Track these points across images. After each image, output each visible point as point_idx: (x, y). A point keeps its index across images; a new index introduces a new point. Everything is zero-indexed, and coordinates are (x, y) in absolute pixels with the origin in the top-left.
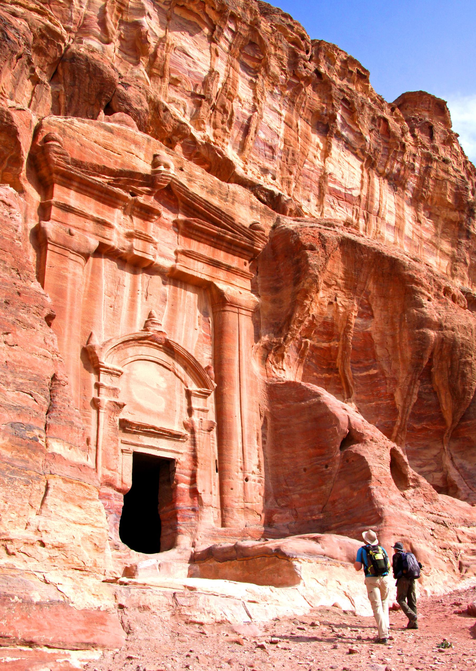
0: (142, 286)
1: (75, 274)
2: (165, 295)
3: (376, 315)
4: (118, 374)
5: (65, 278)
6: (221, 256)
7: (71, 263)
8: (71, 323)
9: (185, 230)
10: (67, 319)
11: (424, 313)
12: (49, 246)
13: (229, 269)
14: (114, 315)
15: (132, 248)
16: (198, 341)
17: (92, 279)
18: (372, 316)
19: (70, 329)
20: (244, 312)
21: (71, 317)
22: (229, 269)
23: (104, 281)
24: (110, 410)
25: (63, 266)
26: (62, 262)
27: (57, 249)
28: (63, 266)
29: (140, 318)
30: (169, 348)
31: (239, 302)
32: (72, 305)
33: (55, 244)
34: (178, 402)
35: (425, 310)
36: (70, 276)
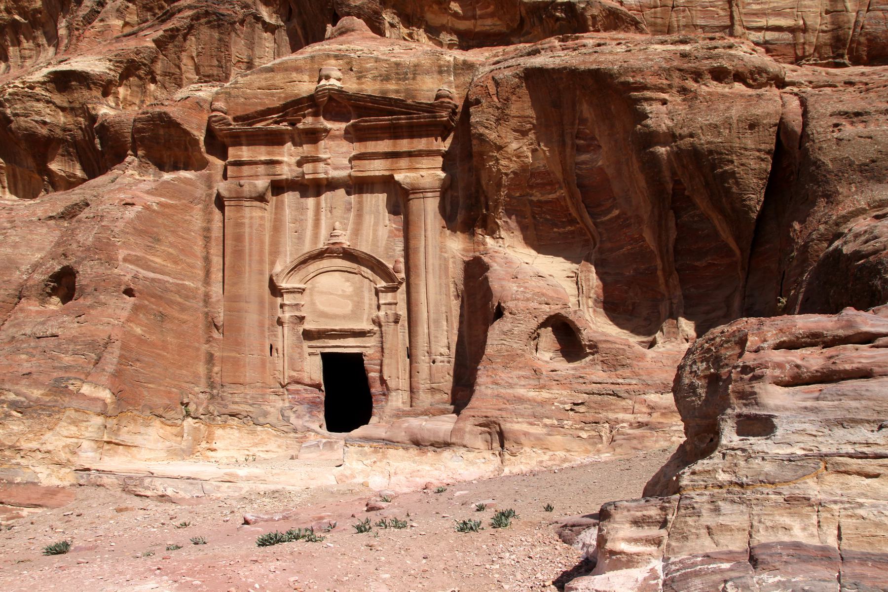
0: (326, 203)
1: (251, 218)
2: (350, 204)
3: (602, 144)
4: (302, 291)
5: (243, 224)
6: (404, 145)
7: (247, 209)
8: (250, 260)
9: (356, 135)
10: (247, 258)
11: (647, 126)
12: (226, 203)
13: (410, 154)
14: (299, 238)
15: (303, 174)
16: (389, 237)
17: (276, 214)
18: (600, 147)
19: (250, 266)
20: (430, 195)
21: (250, 256)
22: (410, 154)
23: (287, 211)
24: (292, 323)
25: (239, 215)
26: (238, 212)
27: (232, 203)
28: (239, 215)
29: (324, 232)
30: (349, 255)
31: (421, 186)
32: (250, 245)
33: (230, 199)
34: (367, 301)
35: (649, 122)
36: (247, 221)
